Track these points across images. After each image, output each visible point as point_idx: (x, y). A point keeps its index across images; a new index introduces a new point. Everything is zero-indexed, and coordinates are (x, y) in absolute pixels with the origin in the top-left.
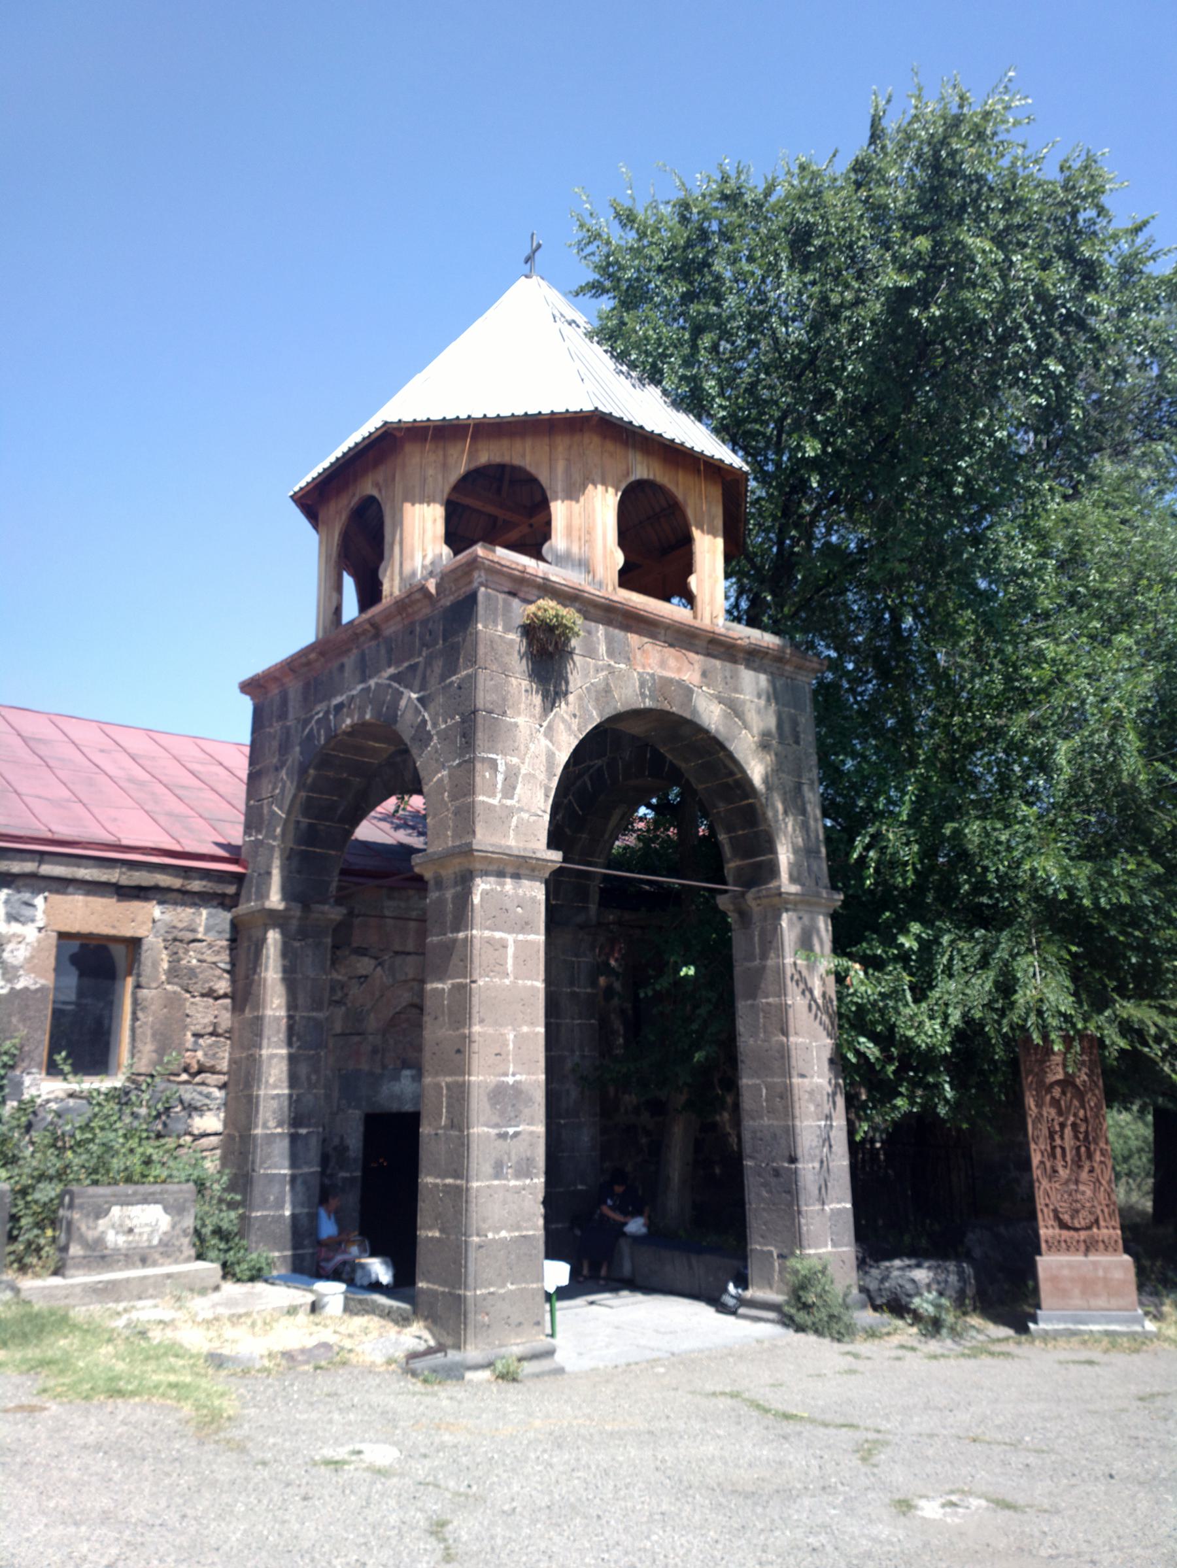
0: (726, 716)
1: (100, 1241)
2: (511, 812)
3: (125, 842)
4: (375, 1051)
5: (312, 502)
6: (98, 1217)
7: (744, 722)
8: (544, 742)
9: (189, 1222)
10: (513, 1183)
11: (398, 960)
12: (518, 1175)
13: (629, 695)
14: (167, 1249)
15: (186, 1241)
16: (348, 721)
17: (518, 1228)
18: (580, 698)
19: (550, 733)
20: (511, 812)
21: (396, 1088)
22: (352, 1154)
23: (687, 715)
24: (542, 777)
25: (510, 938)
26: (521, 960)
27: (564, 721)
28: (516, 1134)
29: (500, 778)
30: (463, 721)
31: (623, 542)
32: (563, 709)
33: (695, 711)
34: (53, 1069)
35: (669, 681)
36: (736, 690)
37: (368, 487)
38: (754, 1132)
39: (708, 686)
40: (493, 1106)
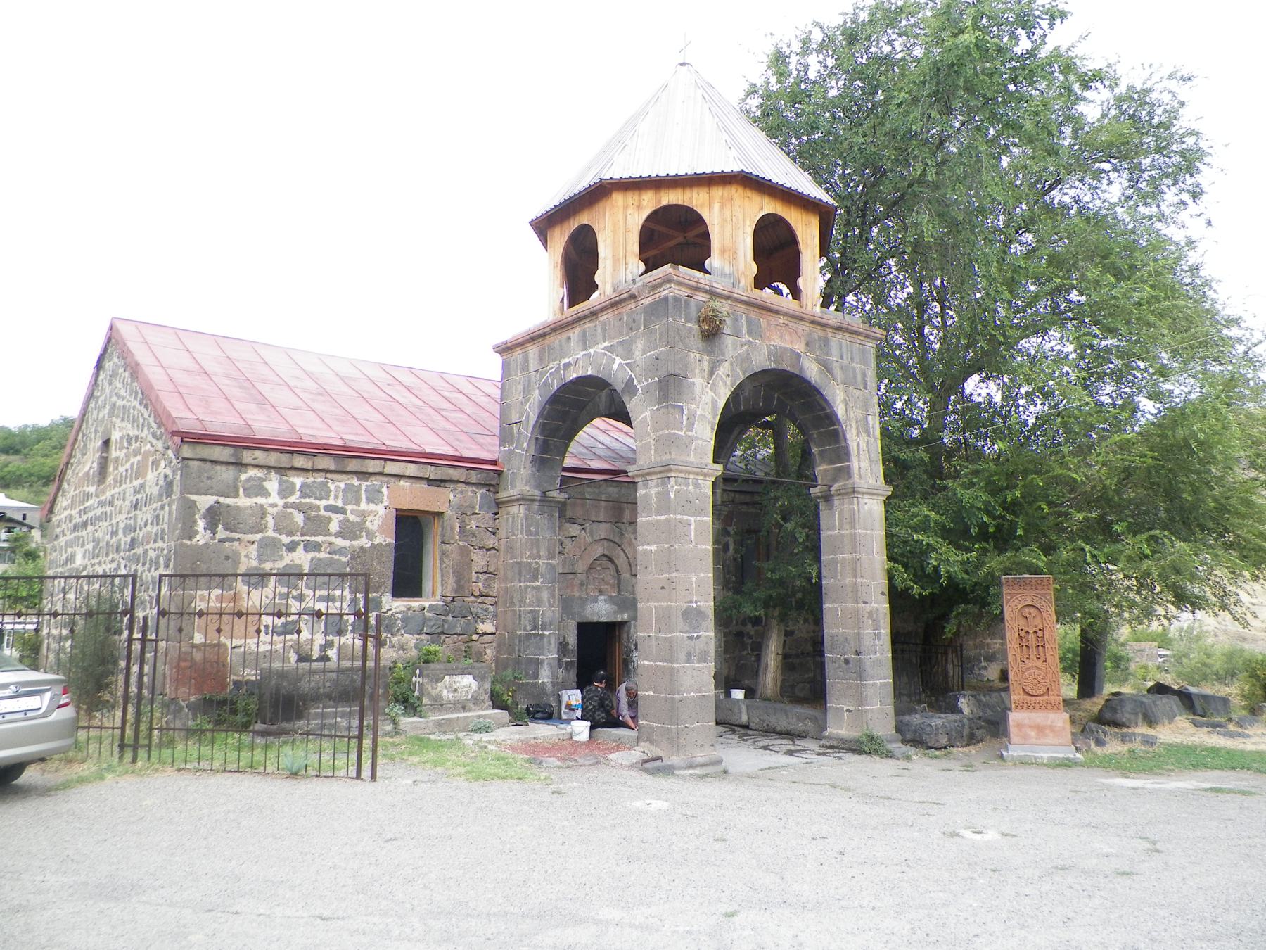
0: (821, 372)
1: (439, 696)
2: (692, 439)
3: (428, 451)
4: (582, 584)
5: (544, 226)
6: (437, 681)
8: (711, 393)
9: (488, 686)
11: (595, 526)
12: (699, 662)
13: (761, 361)
14: (476, 701)
15: (487, 697)
16: (575, 376)
18: (732, 364)
19: (714, 388)
20: (692, 439)
21: (596, 606)
22: (571, 647)
23: (797, 372)
24: (709, 416)
25: (693, 519)
26: (699, 533)
28: (698, 637)
30: (660, 381)
31: (757, 257)
32: (723, 370)
33: (801, 369)
34: (398, 593)
35: (786, 349)
37: (584, 219)
38: (833, 637)
40: (685, 620)
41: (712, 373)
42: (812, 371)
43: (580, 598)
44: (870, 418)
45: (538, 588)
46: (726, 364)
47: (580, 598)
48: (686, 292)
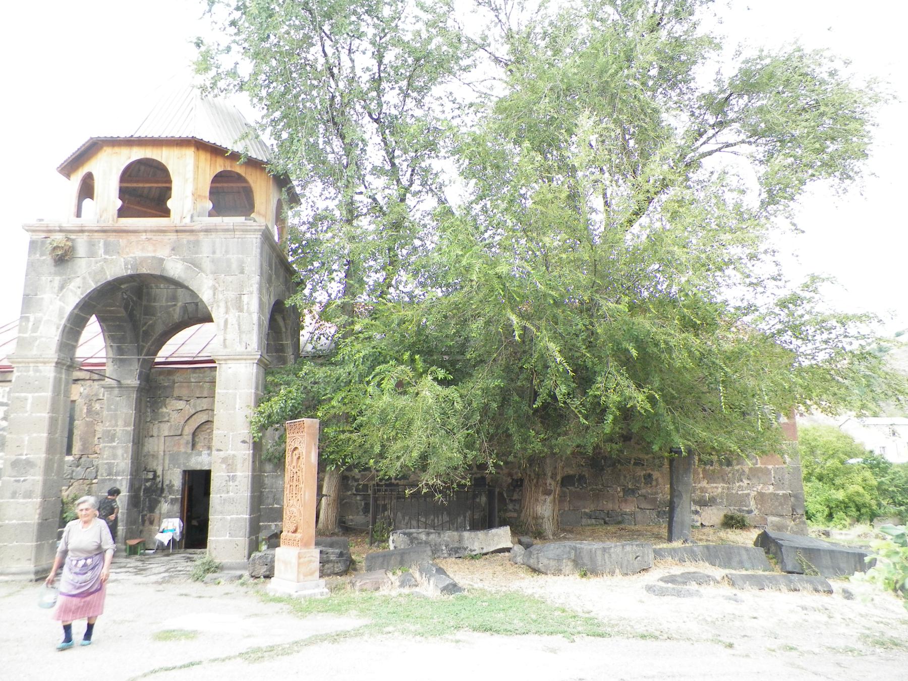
0: (188, 268)
2: (36, 339)
7: (200, 269)
10: (21, 500)
11: (199, 401)
12: (24, 498)
17: (22, 519)
18: (84, 278)
20: (36, 339)
21: (200, 459)
22: (176, 488)
25: (30, 396)
27: (72, 291)
28: (24, 481)
29: (30, 324)
32: (72, 286)
36: (196, 253)
39: (175, 255)
41: (62, 288)
42: (175, 269)
43: (186, 453)
44: (245, 299)
45: (114, 448)
46: (78, 280)
47: (186, 453)
48: (44, 235)
